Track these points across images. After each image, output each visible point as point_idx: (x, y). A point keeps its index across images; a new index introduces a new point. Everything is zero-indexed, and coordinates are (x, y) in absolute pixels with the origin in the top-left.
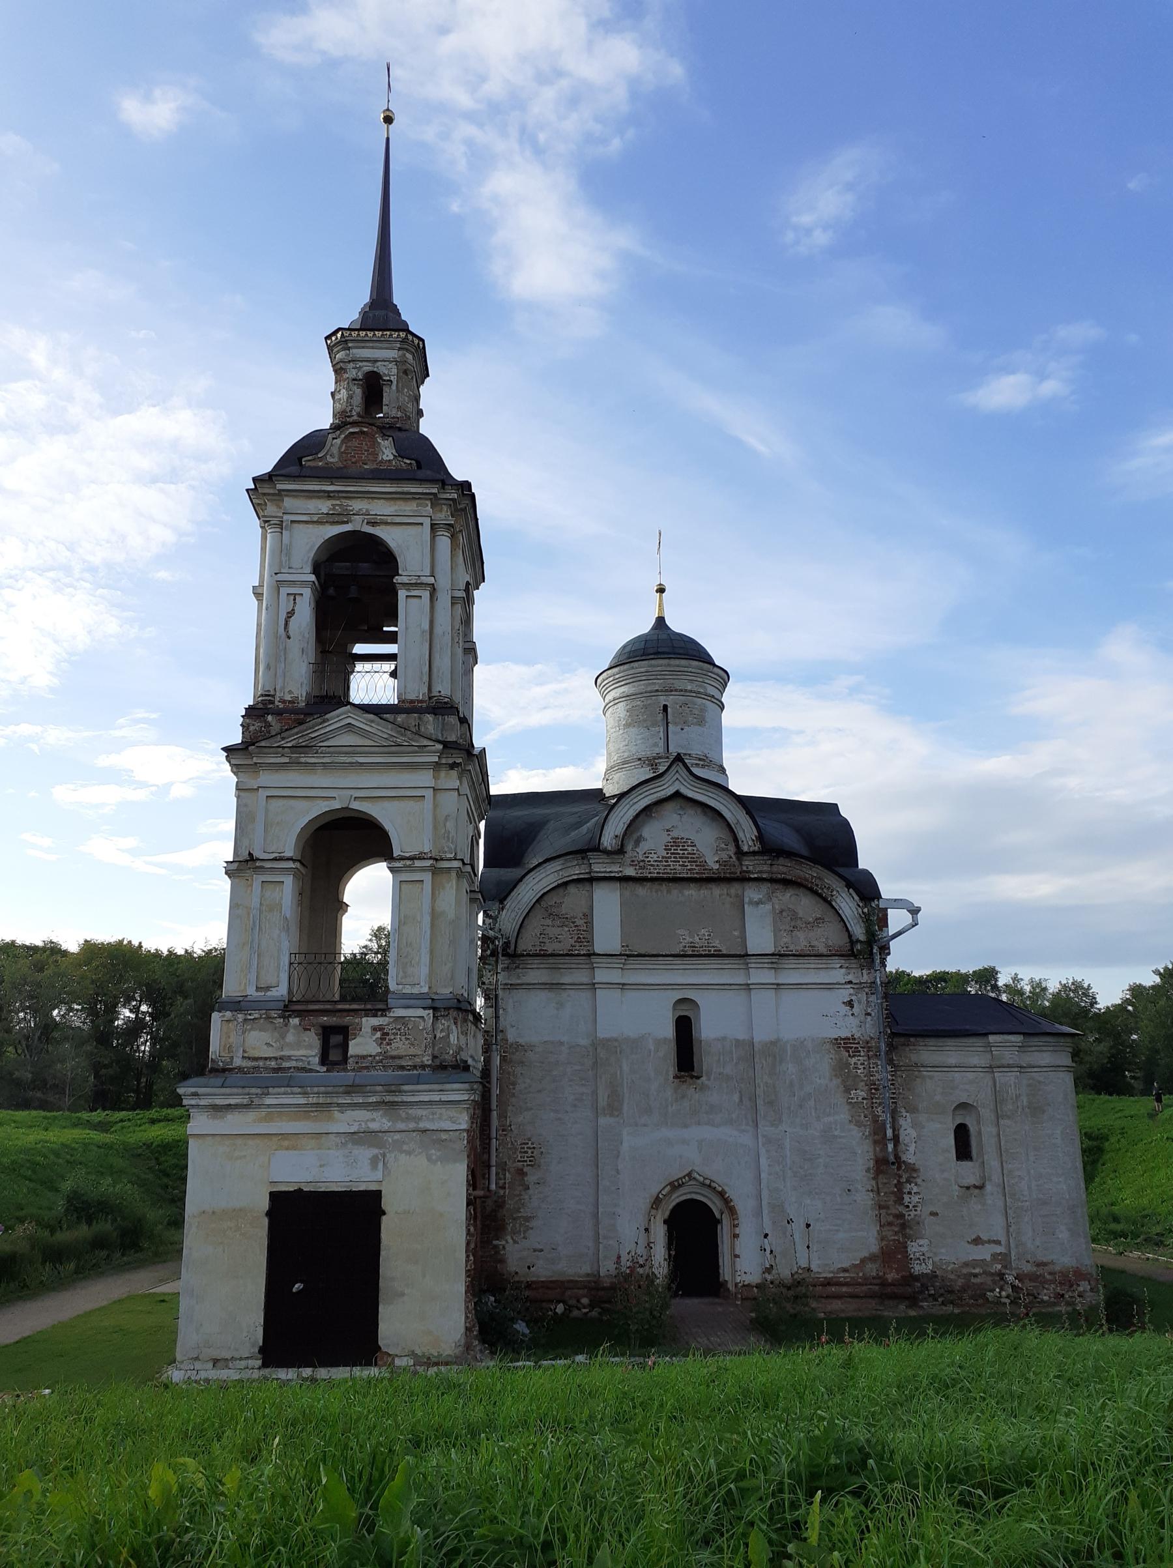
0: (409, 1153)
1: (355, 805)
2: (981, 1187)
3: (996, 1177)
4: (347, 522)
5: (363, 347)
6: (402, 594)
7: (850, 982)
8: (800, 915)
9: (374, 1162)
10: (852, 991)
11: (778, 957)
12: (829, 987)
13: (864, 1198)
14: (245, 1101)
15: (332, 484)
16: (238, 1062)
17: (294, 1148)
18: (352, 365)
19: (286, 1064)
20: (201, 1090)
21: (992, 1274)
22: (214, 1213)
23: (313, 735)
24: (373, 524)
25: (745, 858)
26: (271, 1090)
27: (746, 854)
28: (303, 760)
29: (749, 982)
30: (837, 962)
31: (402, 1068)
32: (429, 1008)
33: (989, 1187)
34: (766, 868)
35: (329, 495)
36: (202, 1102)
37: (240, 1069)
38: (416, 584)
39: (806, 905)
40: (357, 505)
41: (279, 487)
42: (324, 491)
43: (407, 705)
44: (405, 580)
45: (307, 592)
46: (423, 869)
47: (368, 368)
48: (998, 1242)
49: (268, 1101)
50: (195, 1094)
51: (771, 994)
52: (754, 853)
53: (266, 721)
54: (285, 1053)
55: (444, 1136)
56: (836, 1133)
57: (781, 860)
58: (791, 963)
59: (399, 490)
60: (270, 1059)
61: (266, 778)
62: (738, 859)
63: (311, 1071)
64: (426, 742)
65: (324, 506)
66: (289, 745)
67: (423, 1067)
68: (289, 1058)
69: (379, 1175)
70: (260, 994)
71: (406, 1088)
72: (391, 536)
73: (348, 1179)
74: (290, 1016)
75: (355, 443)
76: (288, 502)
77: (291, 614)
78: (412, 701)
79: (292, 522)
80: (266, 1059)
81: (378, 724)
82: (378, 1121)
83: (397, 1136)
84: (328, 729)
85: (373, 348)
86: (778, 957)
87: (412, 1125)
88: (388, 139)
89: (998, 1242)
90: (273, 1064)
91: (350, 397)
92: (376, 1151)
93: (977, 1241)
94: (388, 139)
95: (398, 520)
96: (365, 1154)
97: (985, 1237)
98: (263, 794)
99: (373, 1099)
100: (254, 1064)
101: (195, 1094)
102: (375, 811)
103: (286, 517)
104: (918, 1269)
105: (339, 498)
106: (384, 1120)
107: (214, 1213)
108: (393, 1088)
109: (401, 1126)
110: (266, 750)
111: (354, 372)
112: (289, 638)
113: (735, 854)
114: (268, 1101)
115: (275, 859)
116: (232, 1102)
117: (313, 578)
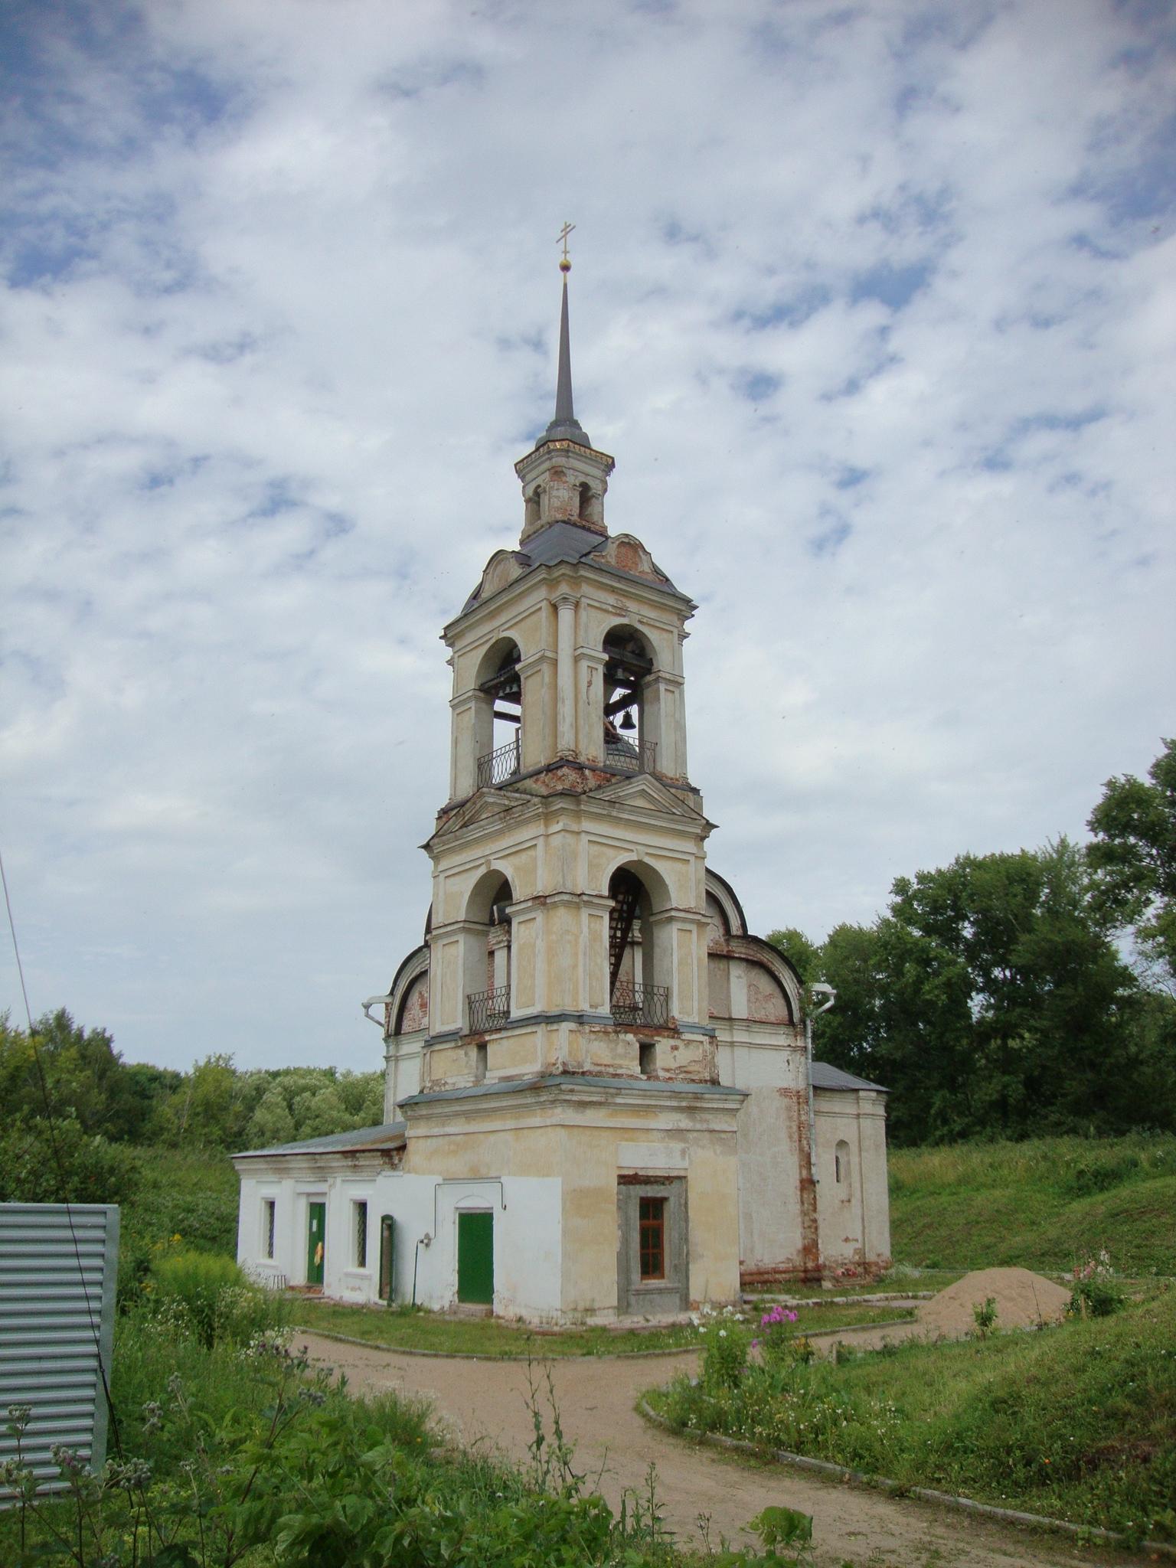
0: (703, 1147)
1: (647, 860)
2: (849, 1201)
3: (858, 1194)
4: (624, 616)
5: (579, 460)
6: (662, 687)
7: (789, 1046)
8: (761, 990)
9: (683, 1152)
10: (789, 1053)
11: (750, 1023)
12: (776, 1048)
13: (795, 1208)
14: (603, 1100)
15: (619, 582)
16: (587, 1067)
17: (632, 1140)
18: (572, 471)
19: (619, 1071)
20: (576, 1088)
21: (854, 1263)
22: (581, 1191)
23: (621, 794)
24: (641, 622)
25: (732, 940)
26: (623, 1091)
27: (734, 936)
28: (614, 814)
29: (735, 1040)
30: (783, 1030)
31: (693, 1081)
32: (706, 1035)
33: (853, 1201)
34: (743, 950)
35: (613, 590)
36: (575, 1098)
37: (591, 1073)
38: (673, 681)
39: (765, 984)
40: (632, 606)
41: (582, 572)
42: (612, 586)
43: (669, 781)
44: (668, 676)
45: (601, 669)
46: (692, 921)
47: (582, 479)
48: (857, 1240)
49: (619, 1100)
50: (572, 1091)
51: (728, 1050)
52: (738, 937)
53: (583, 774)
54: (618, 1062)
55: (723, 1136)
56: (779, 1160)
57: (752, 946)
58: (755, 1028)
59: (662, 601)
60: (609, 1066)
61: (587, 825)
62: (727, 941)
63: (637, 1078)
64: (695, 816)
65: (611, 599)
66: (607, 799)
67: (706, 1081)
68: (621, 1067)
69: (686, 1164)
70: (592, 1010)
71: (707, 1096)
72: (653, 636)
73: (667, 1166)
74: (620, 1031)
75: (623, 550)
76: (586, 589)
77: (590, 684)
78: (672, 779)
79: (588, 604)
80: (605, 1065)
81: (664, 794)
82: (684, 1122)
83: (695, 1134)
84: (631, 791)
85: (586, 463)
86: (750, 1023)
87: (705, 1126)
88: (565, 286)
89: (857, 1240)
90: (611, 1070)
91: (571, 498)
92: (682, 1145)
93: (847, 1240)
94: (565, 286)
95: (658, 624)
96: (677, 1146)
97: (851, 1238)
98: (585, 838)
99: (684, 1104)
100: (598, 1068)
101: (572, 1091)
102: (659, 866)
103: (583, 599)
104: (821, 1260)
105: (618, 594)
106: (687, 1121)
107: (581, 1191)
108: (699, 1096)
109: (698, 1126)
110: (592, 800)
111: (573, 478)
112: (589, 704)
113: (723, 935)
114: (619, 1100)
115: (596, 896)
116: (594, 1099)
117: (606, 657)
